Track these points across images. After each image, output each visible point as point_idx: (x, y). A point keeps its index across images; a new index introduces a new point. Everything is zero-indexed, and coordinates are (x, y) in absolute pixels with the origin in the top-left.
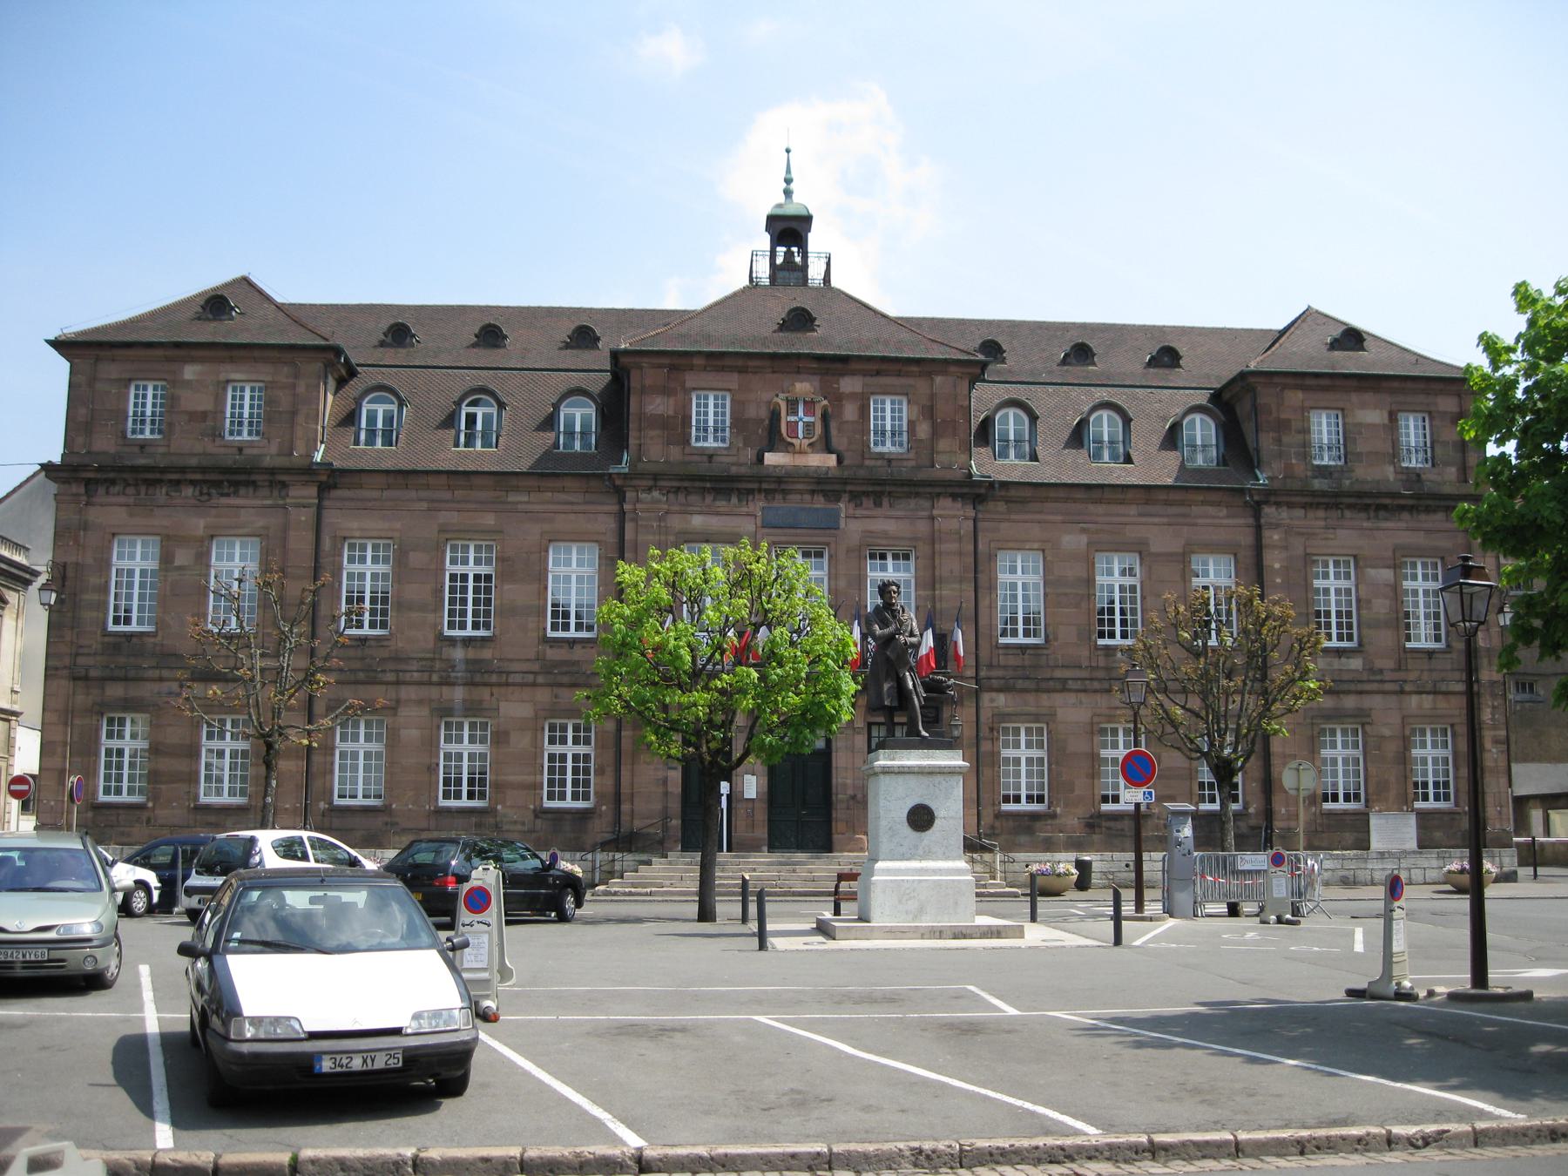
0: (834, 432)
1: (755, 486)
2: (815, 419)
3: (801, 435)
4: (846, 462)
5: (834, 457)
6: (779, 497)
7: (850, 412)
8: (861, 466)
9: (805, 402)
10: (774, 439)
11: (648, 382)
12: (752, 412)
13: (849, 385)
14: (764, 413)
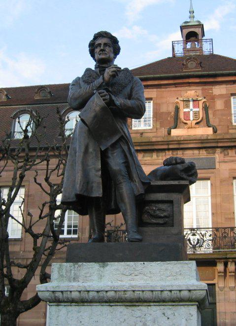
0: (211, 116)
1: (165, 147)
2: (200, 109)
4: (218, 132)
5: (211, 129)
7: (219, 105)
8: (228, 133)
9: (194, 101)
12: (164, 109)
14: (172, 109)
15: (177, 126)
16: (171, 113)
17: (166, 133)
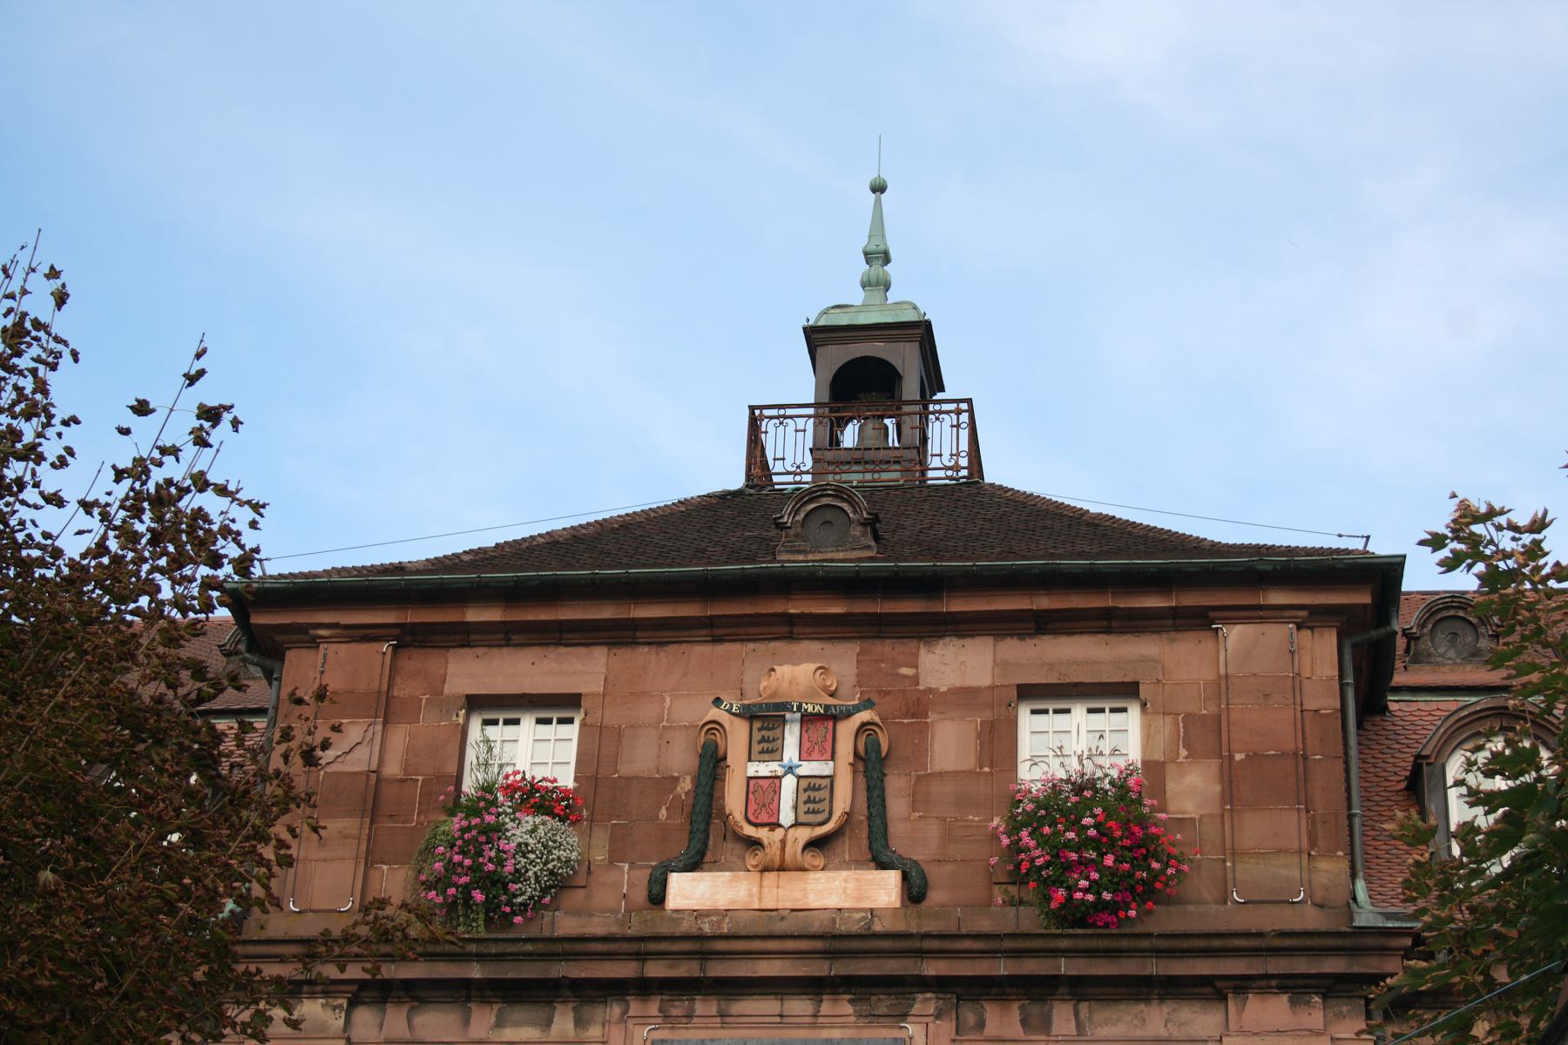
0: (897, 806)
1: (624, 970)
2: (838, 768)
3: (787, 817)
4: (935, 897)
5: (892, 878)
6: (705, 1007)
7: (951, 744)
9: (807, 719)
10: (705, 836)
11: (335, 682)
12: (640, 759)
13: (953, 665)
14: (681, 760)
15: (703, 855)
16: (675, 780)
17: (640, 895)
